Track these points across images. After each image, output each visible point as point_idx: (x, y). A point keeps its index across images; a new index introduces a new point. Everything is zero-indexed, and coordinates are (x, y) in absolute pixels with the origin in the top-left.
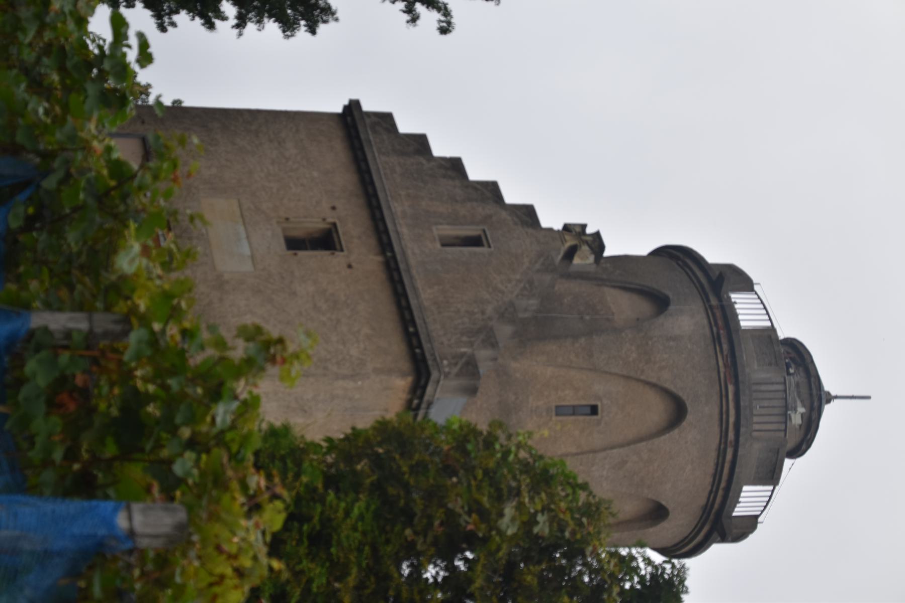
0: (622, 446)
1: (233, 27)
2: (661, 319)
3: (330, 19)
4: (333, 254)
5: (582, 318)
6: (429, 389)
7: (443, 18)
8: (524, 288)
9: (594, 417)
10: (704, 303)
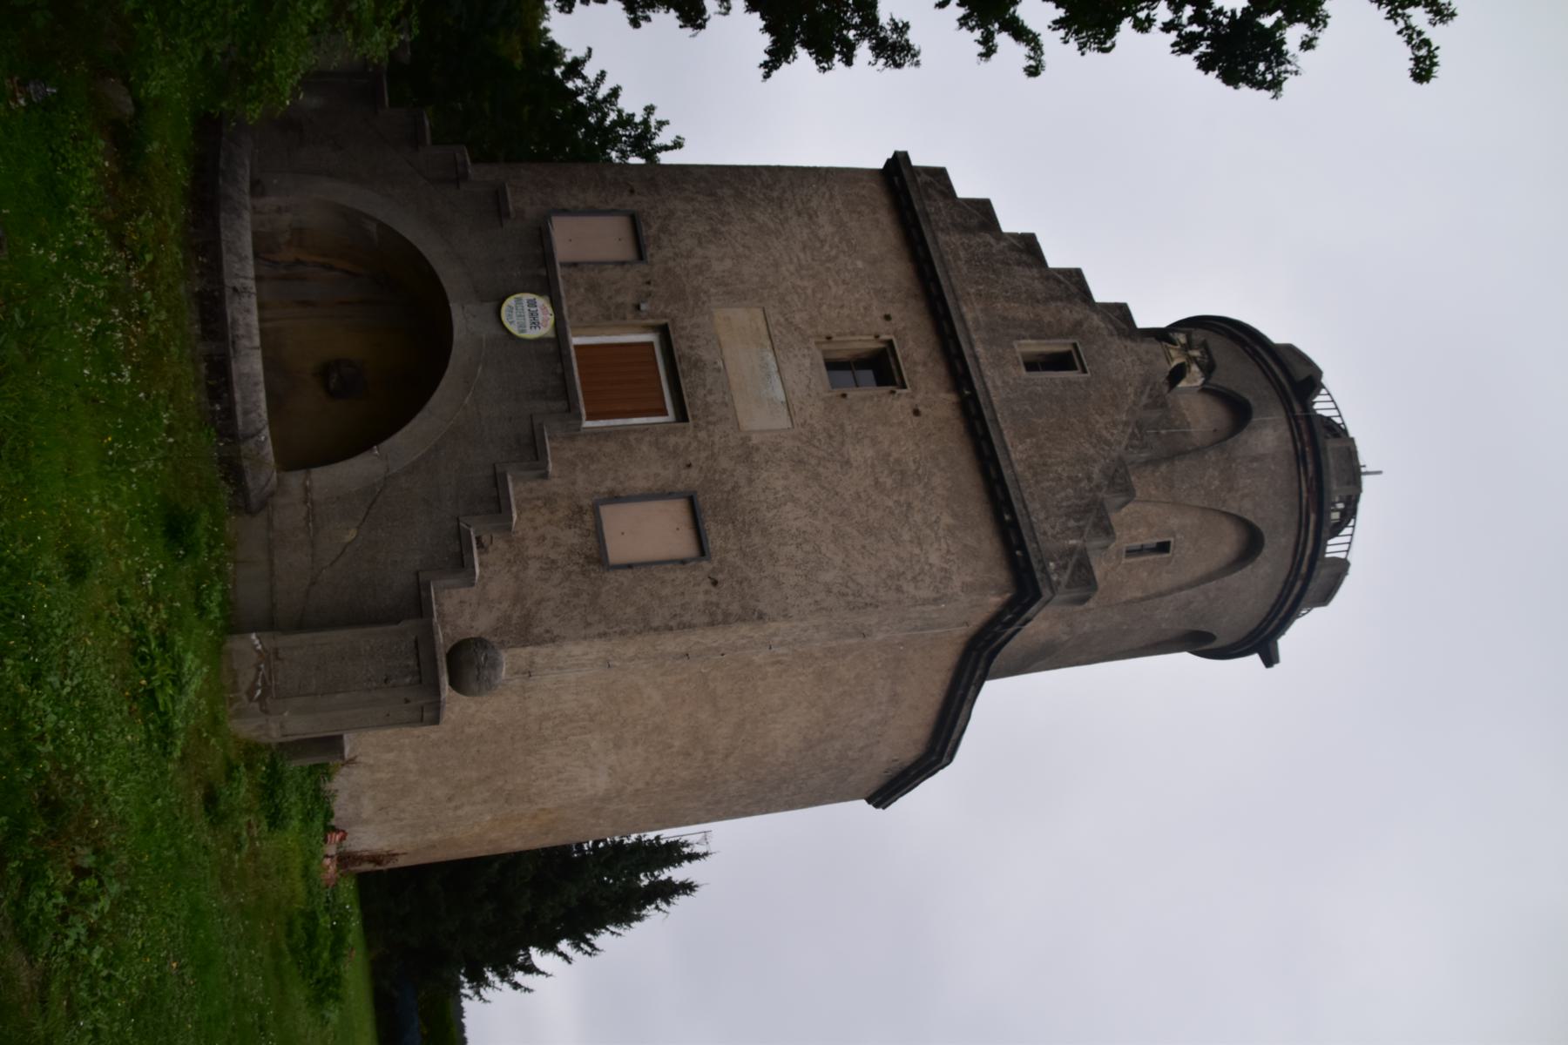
0: (1190, 585)
1: (761, 65)
2: (1244, 436)
3: (907, 64)
4: (893, 392)
5: (1158, 433)
6: (1034, 608)
7: (1032, 54)
8: (1133, 435)
9: (1166, 555)
10: (1287, 412)
